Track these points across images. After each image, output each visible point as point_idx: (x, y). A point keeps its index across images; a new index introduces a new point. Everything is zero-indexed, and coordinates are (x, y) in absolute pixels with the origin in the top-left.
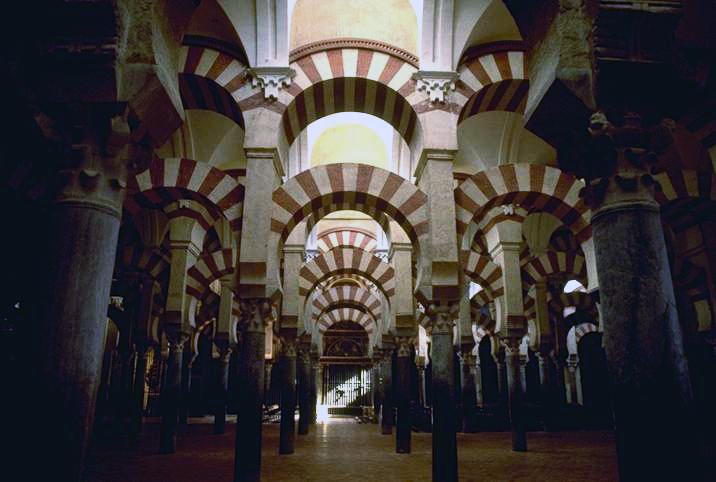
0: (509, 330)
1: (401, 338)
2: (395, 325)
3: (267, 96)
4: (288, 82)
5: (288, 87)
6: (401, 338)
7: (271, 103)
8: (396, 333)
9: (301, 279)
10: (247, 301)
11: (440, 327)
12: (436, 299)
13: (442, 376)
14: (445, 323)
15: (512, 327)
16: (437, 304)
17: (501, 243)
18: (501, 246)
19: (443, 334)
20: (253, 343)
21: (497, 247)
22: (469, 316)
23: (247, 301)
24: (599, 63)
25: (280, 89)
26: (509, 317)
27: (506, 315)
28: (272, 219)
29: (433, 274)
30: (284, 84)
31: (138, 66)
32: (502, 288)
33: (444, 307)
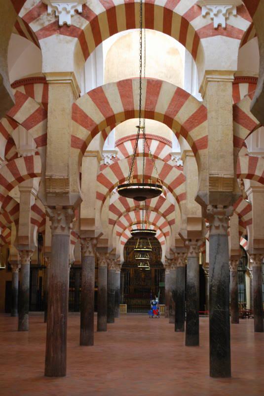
0: (255, 249)
1: (179, 254)
2: (174, 245)
6: (179, 254)
8: (175, 250)
9: (110, 212)
10: (85, 239)
11: (192, 253)
12: (190, 238)
13: (191, 281)
14: (194, 251)
15: (257, 247)
16: (190, 240)
17: (251, 187)
18: (251, 189)
19: (193, 257)
20: (88, 262)
21: (249, 189)
22: (238, 234)
23: (85, 239)
24: (210, 191)
26: (254, 240)
27: (253, 238)
28: (97, 192)
29: (187, 224)
31: (75, 193)
32: (251, 219)
33: (194, 242)
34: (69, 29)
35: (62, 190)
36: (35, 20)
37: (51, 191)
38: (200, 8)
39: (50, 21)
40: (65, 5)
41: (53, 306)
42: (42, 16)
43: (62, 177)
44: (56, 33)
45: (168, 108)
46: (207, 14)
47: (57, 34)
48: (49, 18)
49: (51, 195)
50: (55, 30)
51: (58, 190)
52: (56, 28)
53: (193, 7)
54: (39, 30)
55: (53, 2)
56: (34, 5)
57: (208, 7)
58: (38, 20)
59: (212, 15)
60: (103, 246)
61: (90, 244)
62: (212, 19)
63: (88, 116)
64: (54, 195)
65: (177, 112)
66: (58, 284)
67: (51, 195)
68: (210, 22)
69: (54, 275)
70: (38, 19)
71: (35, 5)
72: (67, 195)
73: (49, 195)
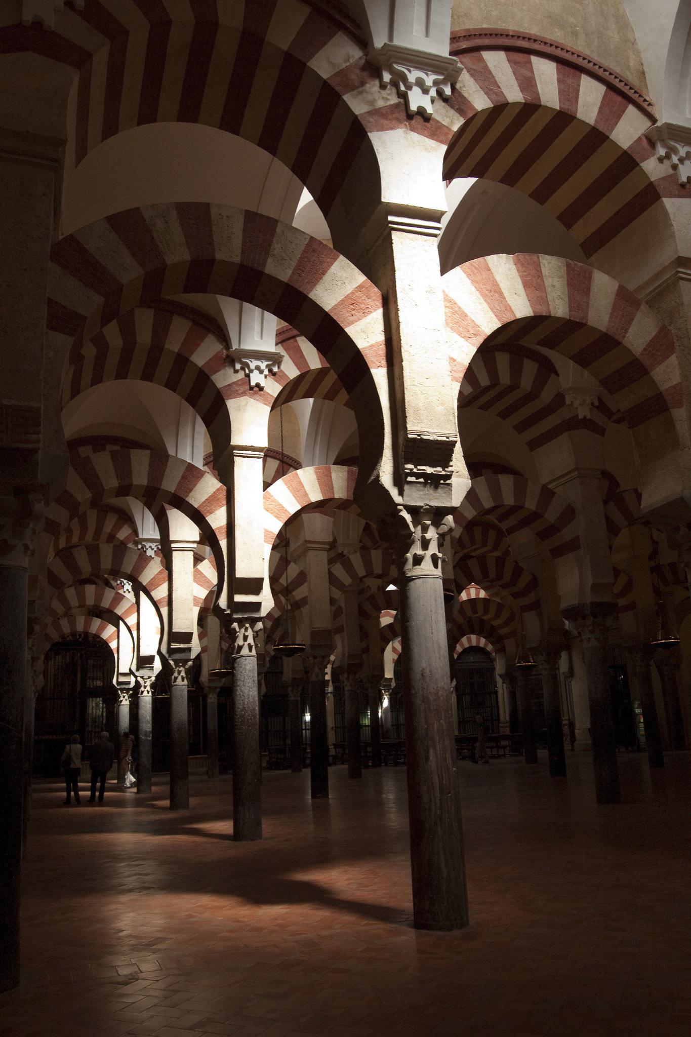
3: (253, 384)
4: (275, 369)
5: (274, 374)
6: (315, 658)
7: (256, 393)
25: (266, 377)
30: (270, 371)
34: (428, 125)
35: (439, 469)
36: (356, 92)
37: (415, 470)
38: (652, 144)
39: (387, 99)
40: (421, 74)
41: (435, 748)
42: (368, 85)
43: (445, 439)
44: (403, 125)
45: (610, 322)
46: (668, 156)
47: (404, 129)
48: (384, 93)
49: (413, 479)
50: (399, 121)
51: (429, 470)
52: (403, 115)
53: (640, 138)
54: (365, 113)
55: (396, 63)
56: (348, 60)
57: (672, 143)
58: (361, 93)
59: (675, 159)
60: (182, 646)
61: (250, 630)
62: (675, 167)
63: (466, 315)
64: (422, 480)
65: (626, 331)
66: (440, 693)
67: (413, 479)
68: (671, 172)
69: (427, 672)
70: (361, 89)
71: (352, 61)
72: (448, 482)
73: (410, 479)
